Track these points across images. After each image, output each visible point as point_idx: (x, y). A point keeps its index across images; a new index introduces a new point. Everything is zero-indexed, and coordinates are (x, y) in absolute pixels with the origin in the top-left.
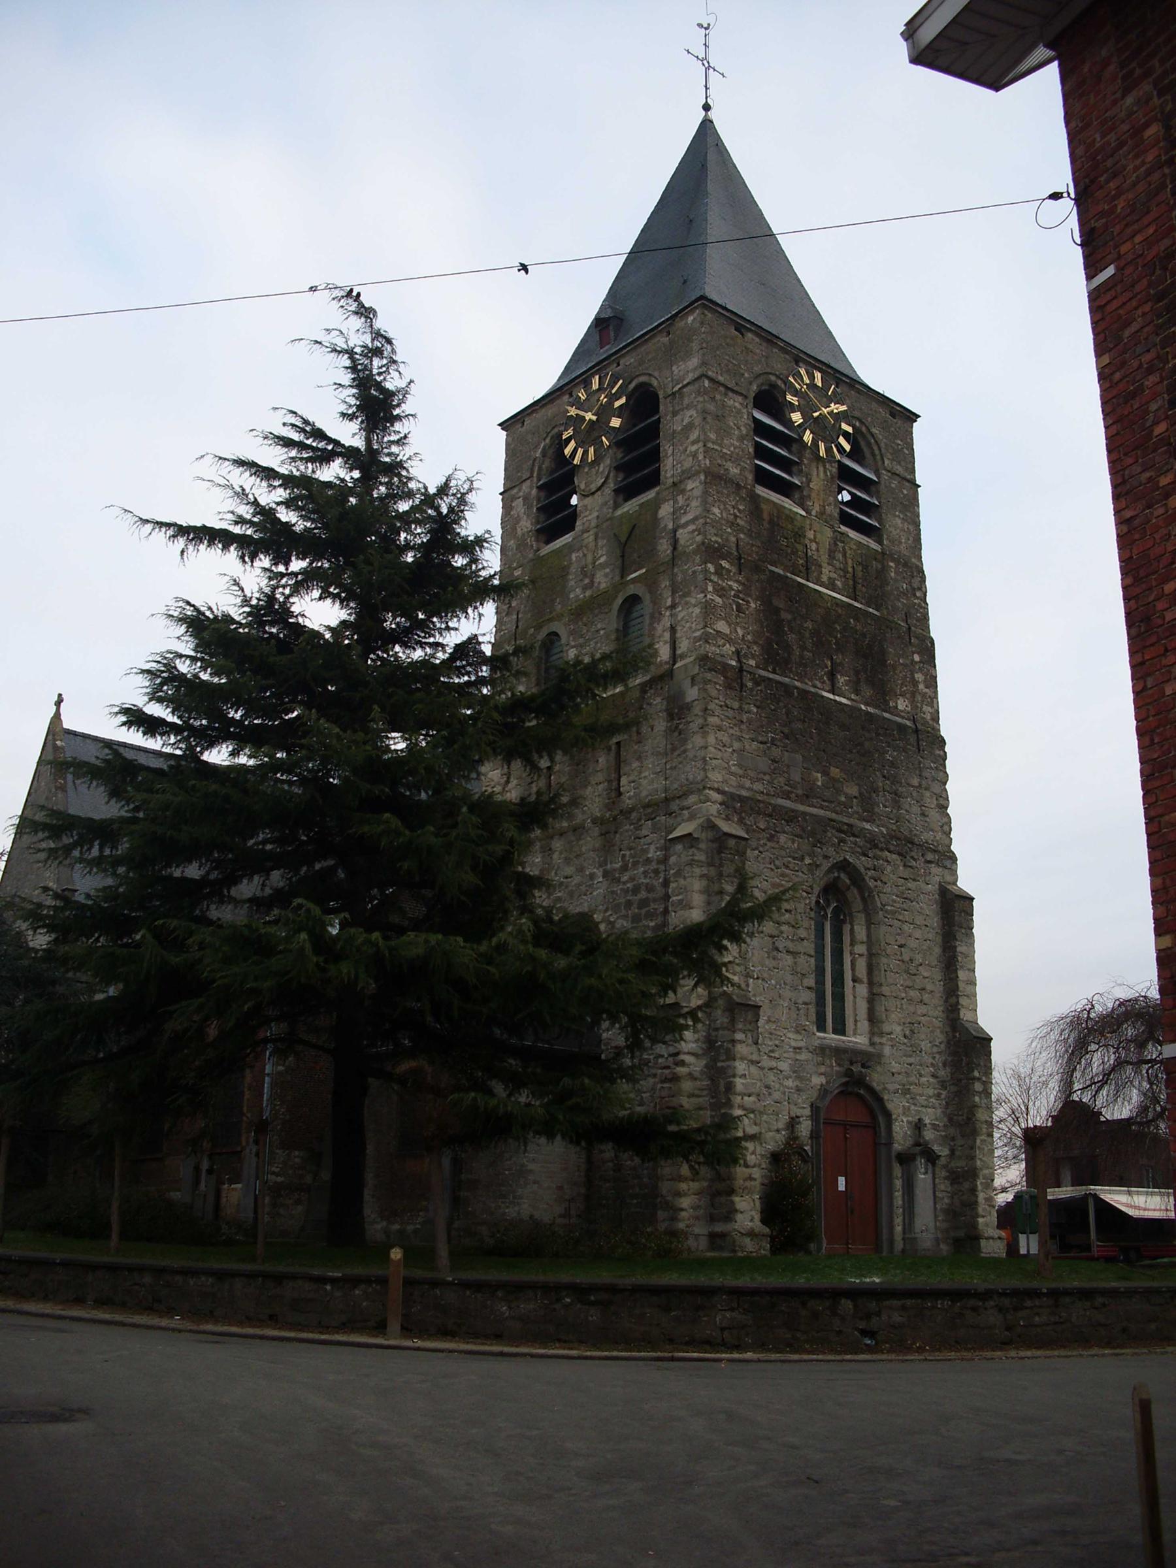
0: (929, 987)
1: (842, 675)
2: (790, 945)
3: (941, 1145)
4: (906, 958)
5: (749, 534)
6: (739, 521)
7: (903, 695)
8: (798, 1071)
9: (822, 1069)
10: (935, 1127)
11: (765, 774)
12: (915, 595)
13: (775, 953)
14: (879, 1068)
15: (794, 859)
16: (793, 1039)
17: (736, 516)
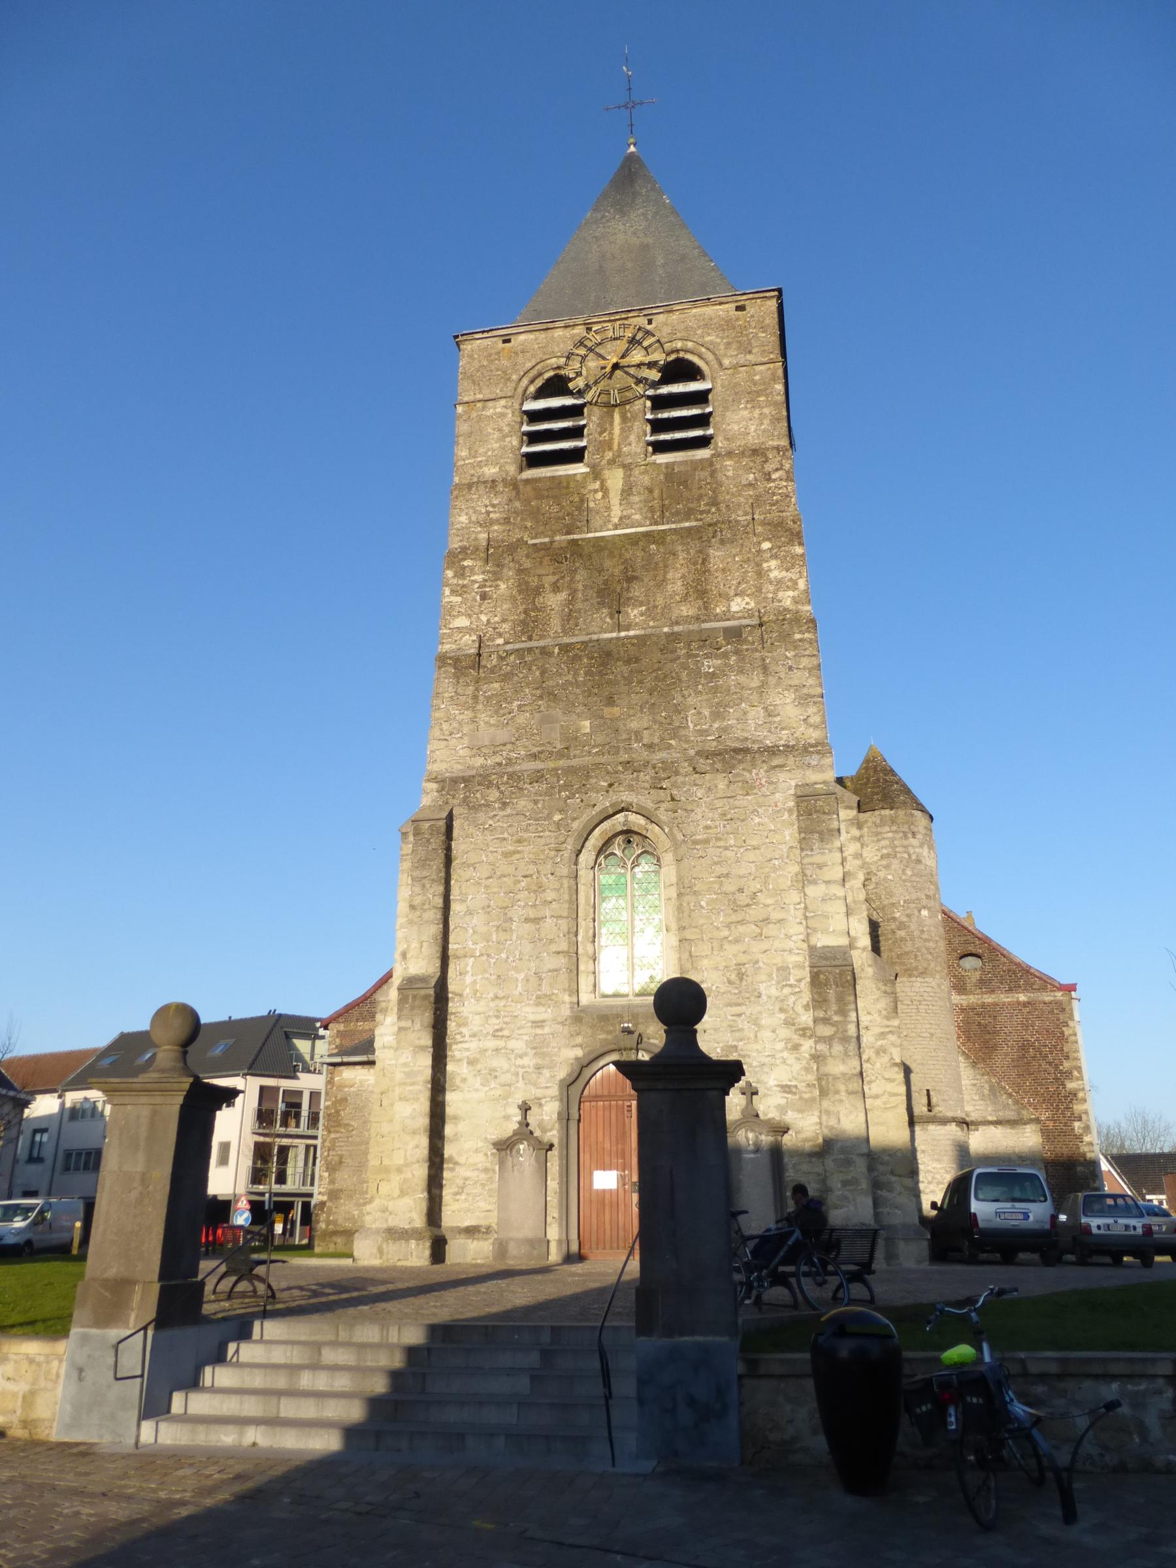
0: (776, 915)
1: (635, 606)
2: (532, 914)
3: (800, 1111)
4: (730, 887)
6: (492, 515)
8: (538, 1047)
9: (579, 1040)
10: (786, 1089)
11: (504, 745)
12: (769, 480)
13: (507, 925)
15: (536, 820)
16: (530, 1012)
17: (488, 513)
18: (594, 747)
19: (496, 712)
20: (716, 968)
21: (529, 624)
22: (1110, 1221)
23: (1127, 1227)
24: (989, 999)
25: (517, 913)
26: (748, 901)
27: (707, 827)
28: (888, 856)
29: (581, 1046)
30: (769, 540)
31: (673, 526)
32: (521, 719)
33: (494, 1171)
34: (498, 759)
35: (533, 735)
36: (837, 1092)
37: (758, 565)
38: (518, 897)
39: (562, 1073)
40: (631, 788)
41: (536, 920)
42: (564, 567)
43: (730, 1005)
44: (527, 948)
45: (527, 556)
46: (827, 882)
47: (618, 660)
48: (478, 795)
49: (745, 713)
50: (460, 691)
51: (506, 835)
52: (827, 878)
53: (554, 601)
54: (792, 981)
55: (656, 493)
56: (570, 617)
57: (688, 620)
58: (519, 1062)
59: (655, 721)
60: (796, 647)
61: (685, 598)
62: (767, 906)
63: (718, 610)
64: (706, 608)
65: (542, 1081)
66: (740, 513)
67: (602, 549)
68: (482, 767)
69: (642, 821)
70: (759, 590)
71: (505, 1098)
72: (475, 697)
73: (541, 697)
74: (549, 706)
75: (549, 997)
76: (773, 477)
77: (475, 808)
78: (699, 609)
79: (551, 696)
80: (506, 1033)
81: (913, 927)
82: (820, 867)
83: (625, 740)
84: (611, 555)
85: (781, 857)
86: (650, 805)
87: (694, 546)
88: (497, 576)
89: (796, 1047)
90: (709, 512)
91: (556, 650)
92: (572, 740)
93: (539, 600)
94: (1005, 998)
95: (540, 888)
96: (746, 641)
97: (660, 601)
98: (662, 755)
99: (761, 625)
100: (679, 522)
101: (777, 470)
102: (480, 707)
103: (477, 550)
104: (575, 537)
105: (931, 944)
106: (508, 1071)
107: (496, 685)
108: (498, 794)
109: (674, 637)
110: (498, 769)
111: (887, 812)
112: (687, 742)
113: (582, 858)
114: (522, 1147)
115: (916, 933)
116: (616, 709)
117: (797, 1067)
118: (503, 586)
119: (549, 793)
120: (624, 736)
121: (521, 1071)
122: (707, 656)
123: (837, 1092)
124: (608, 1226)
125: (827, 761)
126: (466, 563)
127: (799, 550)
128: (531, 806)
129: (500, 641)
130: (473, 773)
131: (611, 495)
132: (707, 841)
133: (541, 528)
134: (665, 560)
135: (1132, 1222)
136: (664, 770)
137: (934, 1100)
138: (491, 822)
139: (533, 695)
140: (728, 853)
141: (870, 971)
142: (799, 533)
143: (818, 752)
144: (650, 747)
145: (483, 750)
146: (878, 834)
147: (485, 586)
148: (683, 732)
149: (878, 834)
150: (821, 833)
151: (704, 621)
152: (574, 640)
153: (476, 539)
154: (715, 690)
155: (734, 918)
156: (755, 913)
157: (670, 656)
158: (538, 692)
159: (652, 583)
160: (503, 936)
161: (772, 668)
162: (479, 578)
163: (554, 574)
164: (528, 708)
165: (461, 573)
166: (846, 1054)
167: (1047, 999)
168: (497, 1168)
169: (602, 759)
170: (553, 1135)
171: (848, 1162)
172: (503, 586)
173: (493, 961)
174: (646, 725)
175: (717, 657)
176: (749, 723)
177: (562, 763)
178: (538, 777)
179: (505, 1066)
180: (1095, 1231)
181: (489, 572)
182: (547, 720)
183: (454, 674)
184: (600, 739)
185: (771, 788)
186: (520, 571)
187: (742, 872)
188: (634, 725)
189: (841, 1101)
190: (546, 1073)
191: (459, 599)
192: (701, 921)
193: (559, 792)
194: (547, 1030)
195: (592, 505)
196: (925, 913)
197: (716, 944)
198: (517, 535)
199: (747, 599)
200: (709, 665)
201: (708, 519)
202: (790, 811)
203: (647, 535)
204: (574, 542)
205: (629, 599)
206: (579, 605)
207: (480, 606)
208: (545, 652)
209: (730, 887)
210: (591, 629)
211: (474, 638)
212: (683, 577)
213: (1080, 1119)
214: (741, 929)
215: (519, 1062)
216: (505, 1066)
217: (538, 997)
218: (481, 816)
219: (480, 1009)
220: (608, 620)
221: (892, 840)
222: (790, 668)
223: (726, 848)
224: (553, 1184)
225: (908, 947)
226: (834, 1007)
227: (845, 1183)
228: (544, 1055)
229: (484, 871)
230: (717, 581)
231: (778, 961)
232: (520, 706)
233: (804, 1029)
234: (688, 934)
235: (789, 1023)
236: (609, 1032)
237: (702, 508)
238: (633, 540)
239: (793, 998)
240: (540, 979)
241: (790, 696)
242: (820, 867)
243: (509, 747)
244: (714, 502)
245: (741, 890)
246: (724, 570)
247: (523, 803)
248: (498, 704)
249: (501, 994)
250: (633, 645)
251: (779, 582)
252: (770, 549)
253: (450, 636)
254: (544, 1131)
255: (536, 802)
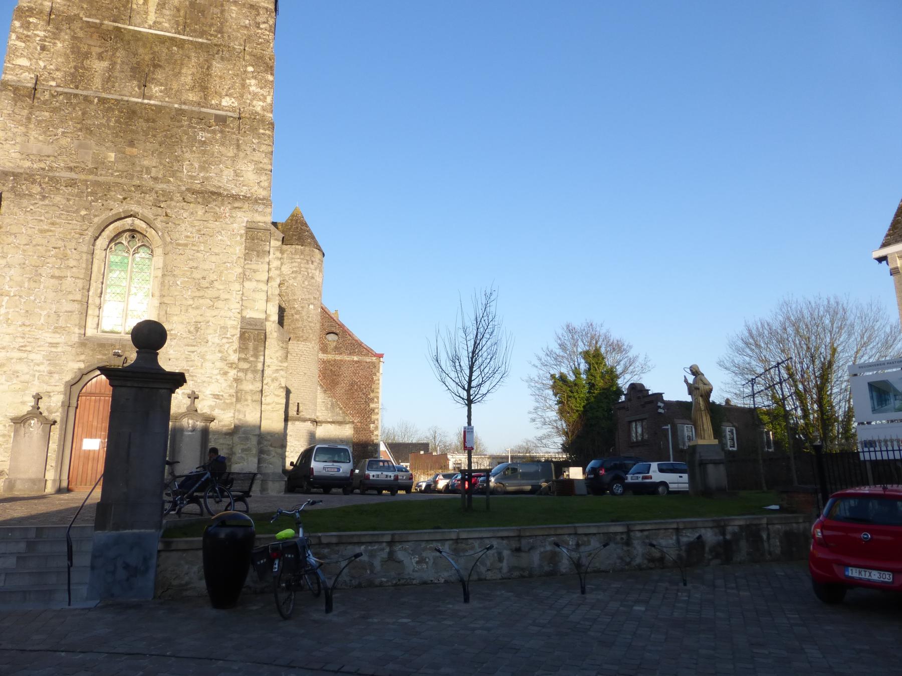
0: (224, 296)
1: (156, 85)
2: (57, 273)
3: (223, 410)
4: (197, 275)
8: (52, 359)
9: (83, 357)
10: (216, 396)
11: (48, 156)
12: (258, 27)
15: (68, 212)
16: (48, 337)
18: (116, 171)
19: (45, 133)
20: (182, 323)
21: (78, 76)
22: (379, 473)
23: (387, 476)
24: (338, 357)
25: (45, 271)
26: (207, 285)
27: (187, 237)
28: (296, 272)
29: (83, 361)
30: (253, 66)
31: (191, 39)
32: (64, 142)
33: (10, 436)
34: (42, 165)
35: (71, 154)
36: (246, 400)
37: (243, 80)
38: (48, 261)
39: (68, 377)
40: (138, 203)
41: (60, 278)
42: (108, 44)
43: (188, 345)
44: (51, 295)
45: (81, 28)
46: (258, 281)
47: (140, 117)
48: (24, 187)
49: (221, 171)
50: (16, 111)
51: (43, 218)
52: (258, 278)
53: (99, 66)
54: (228, 336)
55: (182, 13)
56: (109, 80)
57: (192, 103)
58: (37, 368)
59: (161, 164)
60: (259, 138)
61: (192, 89)
62: (219, 290)
63: (213, 102)
64: (205, 99)
65: (53, 381)
66: (237, 43)
67: (138, 40)
68: (29, 168)
69: (144, 225)
70: (242, 96)
71: (24, 391)
72: (29, 119)
73: (80, 130)
74: (85, 138)
75: (64, 328)
76: (262, 26)
77: (21, 196)
78: (201, 98)
79: (89, 131)
80: (28, 348)
81: (304, 313)
82: (255, 271)
83: (139, 171)
84: (144, 45)
85: (232, 262)
86: (151, 216)
87: (203, 57)
88: (55, 36)
89: (226, 373)
90: (216, 36)
91: (96, 100)
92: (99, 164)
93: (87, 63)
94: (347, 358)
95: (65, 257)
96: (228, 126)
97: (175, 86)
98: (164, 186)
99: (240, 118)
100: (195, 37)
101: (264, 23)
102: (32, 126)
103: (41, 12)
104: (120, 25)
105: (312, 324)
106: (27, 373)
107: (47, 114)
108: (39, 189)
109: (181, 112)
110: (41, 172)
111: (300, 247)
112: (181, 181)
113: (98, 242)
114: (32, 422)
115: (305, 317)
116: (135, 150)
117: (224, 384)
118: (59, 45)
119: (79, 195)
120: (138, 169)
121: (37, 374)
122: (202, 130)
123: (246, 400)
124: (89, 472)
125: (268, 210)
126: (31, 20)
127: (270, 78)
128: (64, 201)
129: (53, 83)
130: (22, 171)
131: (150, 4)
132: (186, 245)
133: (94, 12)
134: (182, 59)
135: (389, 474)
136: (163, 196)
137: (301, 408)
138: (32, 207)
139: (74, 127)
140: (199, 255)
141: (275, 335)
142: (272, 67)
143: (264, 204)
144: (155, 179)
145: (31, 157)
146: (293, 258)
147: (45, 41)
148: (179, 174)
149: (293, 258)
150: (258, 252)
151: (203, 107)
152: (110, 96)
153: (41, 4)
154: (204, 152)
155: (197, 294)
156: (211, 293)
157: (177, 124)
158: (79, 126)
159: (171, 73)
160: (33, 285)
161: (243, 147)
162: (42, 34)
163: (100, 47)
164: (69, 135)
165: (27, 26)
166: (254, 379)
167: (368, 360)
168: (12, 434)
169: (123, 181)
170: (57, 416)
171: (247, 439)
172: (59, 45)
173: (23, 301)
174: (154, 164)
175: (208, 132)
176: (223, 178)
177: (91, 177)
178: (72, 183)
179: (26, 369)
180: (371, 478)
181: (49, 31)
182: (81, 146)
183: (13, 98)
184: (121, 167)
185: (232, 220)
186: (74, 38)
187: (206, 267)
188: (146, 163)
189: (248, 405)
190: (56, 376)
191: (23, 45)
192: (176, 293)
193: (87, 196)
194: (59, 349)
195: (134, 6)
196: (311, 307)
197: (183, 308)
198: (74, 11)
199: (233, 100)
200: (202, 136)
201: (215, 41)
202: (241, 236)
203: (172, 39)
204: (118, 29)
205: (153, 79)
206: (116, 74)
207: (39, 54)
208: (86, 99)
209: (197, 275)
210: (124, 92)
211: (33, 76)
212: (193, 74)
213: (374, 423)
214: (201, 301)
215: (37, 368)
216: (26, 369)
217: (56, 328)
218: (25, 202)
219: (10, 332)
220: (136, 89)
221: (300, 263)
222: (254, 150)
223: (198, 251)
224: (53, 446)
225: (299, 324)
226: (251, 353)
227: (243, 450)
228: (55, 365)
229: (23, 240)
230: (215, 84)
231: (222, 323)
232: (63, 133)
233: (232, 364)
234: (166, 300)
235: (223, 359)
236: (105, 355)
237: (212, 32)
238: (162, 40)
239: (227, 345)
240: (59, 316)
241: (251, 167)
242: (255, 271)
243: (52, 158)
244: (220, 31)
245: (204, 278)
246: (220, 77)
247: (58, 199)
248: (46, 127)
249: (27, 323)
250: (152, 110)
251: (255, 95)
252: (253, 72)
253: (13, 70)
254: (50, 412)
255: (68, 200)
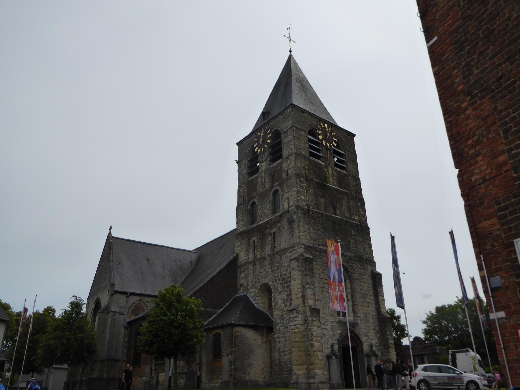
0: (370, 302)
5: (309, 170)
7: (356, 215)
14: (357, 328)
16: (331, 319)
93: (319, 199)
